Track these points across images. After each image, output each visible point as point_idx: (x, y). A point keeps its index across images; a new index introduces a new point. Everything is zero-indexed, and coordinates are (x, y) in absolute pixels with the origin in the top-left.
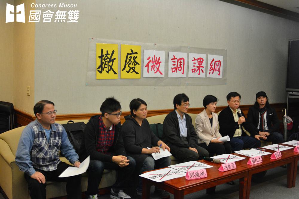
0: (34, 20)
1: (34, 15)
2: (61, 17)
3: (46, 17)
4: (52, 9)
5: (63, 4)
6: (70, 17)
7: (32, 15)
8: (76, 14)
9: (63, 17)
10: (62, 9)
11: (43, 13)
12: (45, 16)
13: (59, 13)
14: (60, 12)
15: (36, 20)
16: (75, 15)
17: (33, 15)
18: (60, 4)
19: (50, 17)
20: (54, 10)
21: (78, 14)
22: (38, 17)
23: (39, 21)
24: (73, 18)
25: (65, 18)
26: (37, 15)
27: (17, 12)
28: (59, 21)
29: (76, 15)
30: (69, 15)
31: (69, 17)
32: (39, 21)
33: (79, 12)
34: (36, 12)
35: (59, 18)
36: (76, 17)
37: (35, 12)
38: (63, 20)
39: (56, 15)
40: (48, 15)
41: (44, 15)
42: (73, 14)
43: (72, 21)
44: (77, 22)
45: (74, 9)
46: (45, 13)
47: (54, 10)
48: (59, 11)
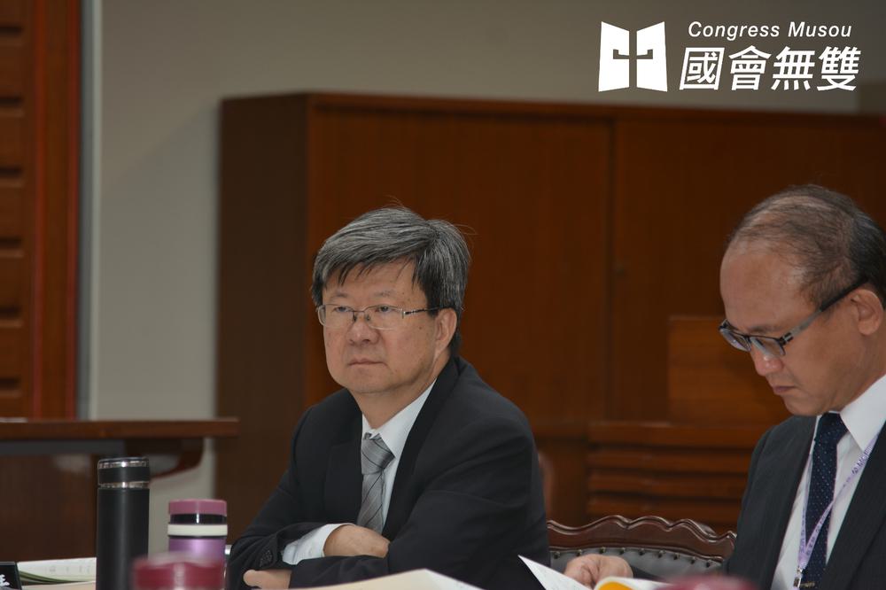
0: (700, 81)
1: (699, 65)
2: (794, 72)
3: (741, 69)
4: (761, 44)
5: (803, 24)
6: (828, 69)
7: (692, 65)
8: (848, 62)
9: (802, 72)
10: (797, 44)
11: (732, 57)
12: (737, 67)
13: (788, 57)
14: (793, 54)
15: (705, 82)
16: (844, 65)
17: (695, 65)
18: (793, 24)
19: (755, 69)
20: (772, 46)
21: (855, 62)
22: (714, 72)
23: (716, 87)
24: (839, 74)
25: (811, 76)
26: (710, 63)
27: (638, 54)
28: (786, 87)
29: (847, 65)
30: (825, 63)
31: (824, 71)
32: (716, 87)
33: (859, 53)
34: (707, 54)
35: (789, 75)
36: (850, 71)
37: (702, 54)
38: (801, 81)
39: (776, 65)
40: (748, 63)
41: (734, 63)
42: (837, 59)
43: (835, 85)
44: (852, 88)
45: (840, 43)
46: (739, 58)
47: (772, 46)
48: (787, 48)
